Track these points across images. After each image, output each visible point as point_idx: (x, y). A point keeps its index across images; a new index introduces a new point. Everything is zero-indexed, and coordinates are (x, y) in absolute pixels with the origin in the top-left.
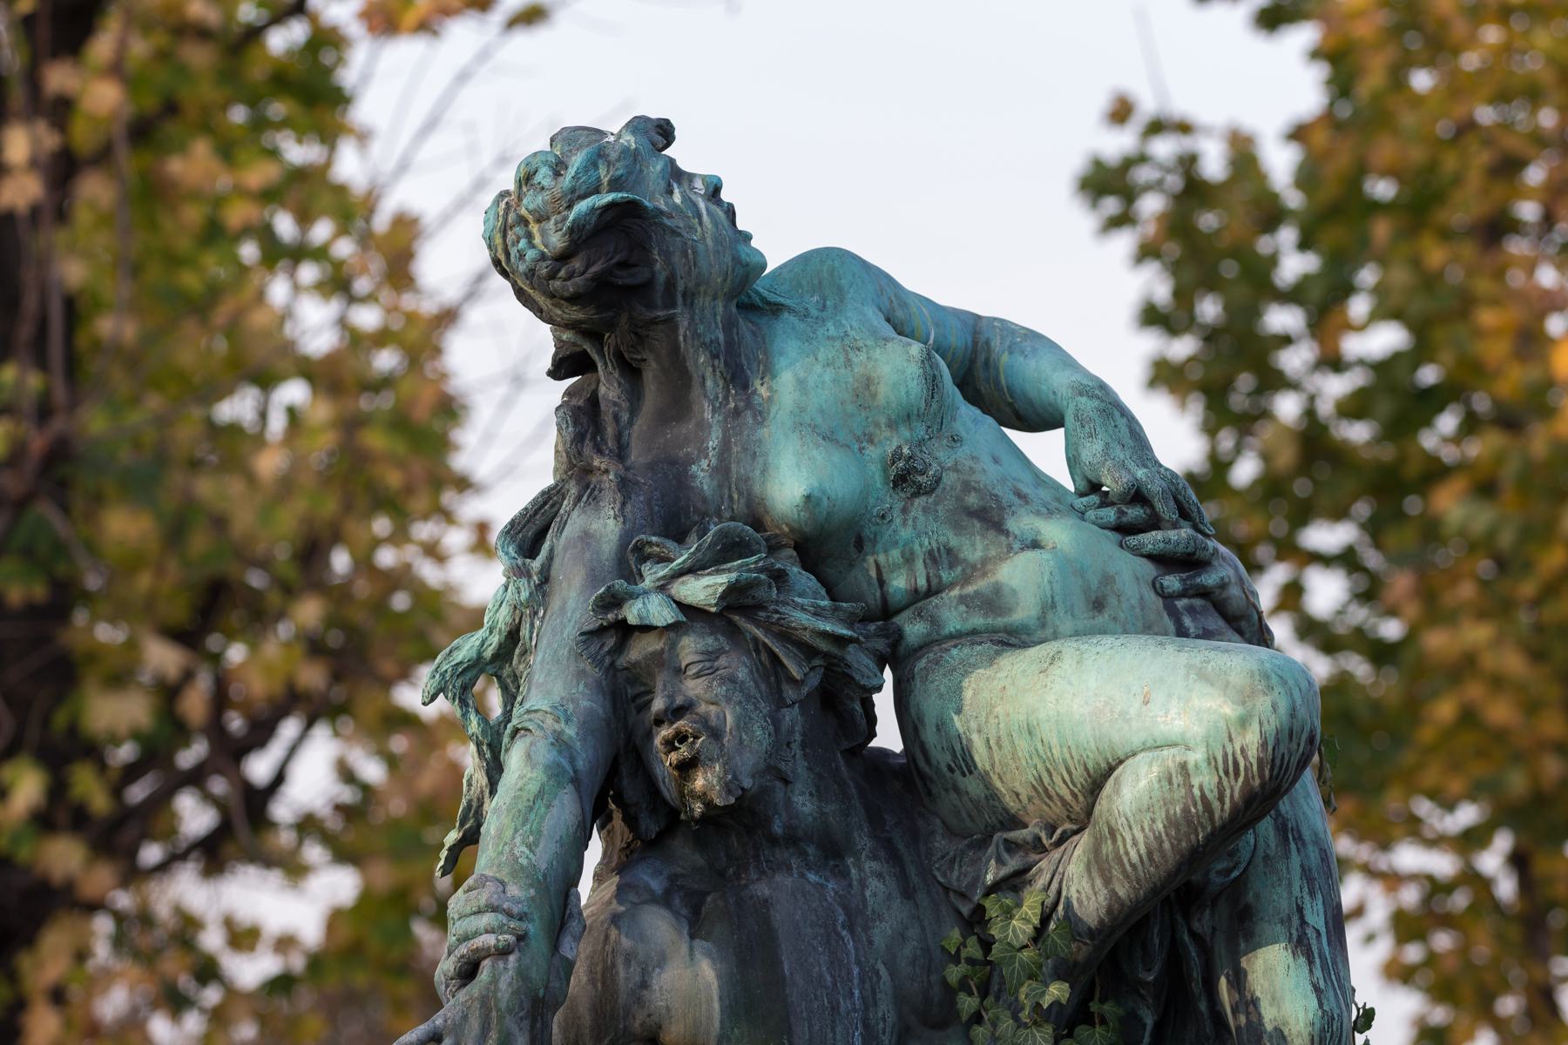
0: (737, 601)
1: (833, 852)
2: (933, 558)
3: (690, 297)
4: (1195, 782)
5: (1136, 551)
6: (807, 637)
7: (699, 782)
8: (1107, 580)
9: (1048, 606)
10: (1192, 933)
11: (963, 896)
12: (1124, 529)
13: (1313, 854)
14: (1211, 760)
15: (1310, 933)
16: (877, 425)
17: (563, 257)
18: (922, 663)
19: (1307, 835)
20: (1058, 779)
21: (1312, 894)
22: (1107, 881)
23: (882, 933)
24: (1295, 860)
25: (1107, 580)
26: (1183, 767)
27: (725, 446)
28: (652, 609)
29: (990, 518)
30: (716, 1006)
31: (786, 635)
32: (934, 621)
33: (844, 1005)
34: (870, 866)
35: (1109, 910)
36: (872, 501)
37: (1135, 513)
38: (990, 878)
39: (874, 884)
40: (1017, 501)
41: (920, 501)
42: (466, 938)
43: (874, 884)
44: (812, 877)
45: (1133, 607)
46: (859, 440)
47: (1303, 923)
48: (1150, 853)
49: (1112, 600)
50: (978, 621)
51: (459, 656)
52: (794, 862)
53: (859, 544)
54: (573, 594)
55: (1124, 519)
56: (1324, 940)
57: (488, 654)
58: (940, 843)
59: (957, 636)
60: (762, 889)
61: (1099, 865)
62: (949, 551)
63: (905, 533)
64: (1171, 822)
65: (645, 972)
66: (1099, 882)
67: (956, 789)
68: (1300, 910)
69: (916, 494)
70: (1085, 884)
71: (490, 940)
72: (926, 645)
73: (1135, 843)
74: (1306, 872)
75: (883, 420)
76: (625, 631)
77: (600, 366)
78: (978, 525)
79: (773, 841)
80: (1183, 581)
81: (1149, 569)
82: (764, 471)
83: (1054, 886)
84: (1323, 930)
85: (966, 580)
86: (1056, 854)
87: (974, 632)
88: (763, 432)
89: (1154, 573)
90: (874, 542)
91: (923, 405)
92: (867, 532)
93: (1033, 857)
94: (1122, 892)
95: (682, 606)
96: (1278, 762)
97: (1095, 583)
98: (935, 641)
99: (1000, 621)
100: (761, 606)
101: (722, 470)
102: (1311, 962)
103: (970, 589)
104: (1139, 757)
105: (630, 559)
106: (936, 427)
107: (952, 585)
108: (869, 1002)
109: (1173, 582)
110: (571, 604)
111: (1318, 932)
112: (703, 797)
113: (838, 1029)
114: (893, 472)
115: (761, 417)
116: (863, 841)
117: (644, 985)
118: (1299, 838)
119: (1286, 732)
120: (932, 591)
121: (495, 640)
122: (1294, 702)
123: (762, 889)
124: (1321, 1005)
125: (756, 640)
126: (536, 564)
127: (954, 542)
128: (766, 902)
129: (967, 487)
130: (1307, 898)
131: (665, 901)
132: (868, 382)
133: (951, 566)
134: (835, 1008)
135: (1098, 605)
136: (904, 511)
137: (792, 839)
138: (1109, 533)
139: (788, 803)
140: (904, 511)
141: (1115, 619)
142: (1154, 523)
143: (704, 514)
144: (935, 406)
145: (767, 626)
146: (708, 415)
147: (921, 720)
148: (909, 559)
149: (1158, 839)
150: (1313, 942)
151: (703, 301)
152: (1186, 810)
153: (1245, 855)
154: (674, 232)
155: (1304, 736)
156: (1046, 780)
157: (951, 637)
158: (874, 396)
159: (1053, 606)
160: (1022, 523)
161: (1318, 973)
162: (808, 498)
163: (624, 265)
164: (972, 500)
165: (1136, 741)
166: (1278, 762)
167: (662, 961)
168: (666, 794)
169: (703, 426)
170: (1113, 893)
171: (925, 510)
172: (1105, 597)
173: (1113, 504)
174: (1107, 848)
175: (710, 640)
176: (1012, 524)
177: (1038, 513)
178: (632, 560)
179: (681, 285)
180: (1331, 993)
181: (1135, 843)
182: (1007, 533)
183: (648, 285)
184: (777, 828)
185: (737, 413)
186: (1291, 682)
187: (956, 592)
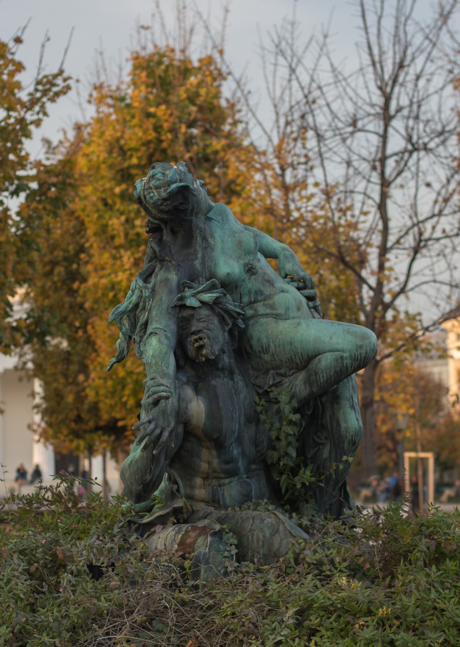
0: (217, 302)
1: (231, 373)
2: (256, 293)
3: (197, 214)
4: (345, 362)
5: (302, 294)
6: (233, 313)
7: (204, 352)
8: (300, 302)
9: (287, 309)
10: (321, 401)
11: (260, 387)
12: (299, 289)
14: (351, 356)
17: (165, 200)
18: (252, 322)
20: (297, 357)
22: (311, 387)
23: (242, 396)
26: (342, 358)
27: (203, 257)
28: (192, 302)
31: (227, 311)
32: (256, 310)
33: (235, 416)
34: (239, 377)
35: (309, 395)
37: (301, 284)
38: (271, 383)
39: (240, 382)
41: (253, 277)
42: (155, 393)
43: (240, 382)
44: (226, 380)
48: (327, 380)
50: (268, 311)
51: (120, 310)
52: (222, 375)
53: (236, 287)
54: (164, 295)
57: (129, 309)
58: (251, 372)
59: (262, 315)
60: (214, 382)
61: (308, 381)
62: (261, 291)
63: (250, 285)
64: (336, 372)
65: (187, 404)
66: (308, 387)
67: (260, 358)
70: (303, 387)
71: (164, 394)
72: (252, 317)
73: (323, 377)
76: (184, 307)
77: (165, 231)
78: (268, 284)
79: (218, 369)
82: (215, 265)
83: (290, 387)
85: (265, 300)
86: (292, 378)
87: (267, 314)
88: (214, 254)
90: (240, 287)
92: (239, 284)
93: (283, 378)
94: (315, 390)
95: (201, 302)
98: (256, 316)
99: (274, 312)
100: (220, 303)
101: (203, 263)
103: (266, 302)
104: (327, 354)
105: (181, 287)
107: (260, 301)
108: (240, 416)
110: (164, 298)
112: (205, 356)
114: (247, 268)
115: (212, 249)
116: (237, 371)
117: (186, 408)
120: (255, 302)
121: (131, 306)
123: (214, 382)
125: (219, 312)
126: (150, 286)
127: (262, 289)
128: (215, 386)
131: (187, 383)
133: (261, 295)
134: (232, 417)
136: (249, 279)
137: (223, 369)
140: (249, 279)
143: (198, 276)
145: (222, 309)
146: (197, 248)
147: (251, 338)
149: (331, 377)
151: (200, 216)
152: (341, 369)
154: (195, 196)
156: (293, 357)
157: (260, 315)
162: (228, 274)
163: (181, 204)
165: (327, 349)
167: (191, 401)
168: (190, 354)
169: (196, 251)
170: (312, 390)
171: (255, 279)
173: (295, 281)
174: (313, 378)
176: (276, 285)
178: (181, 287)
179: (195, 210)
181: (323, 377)
182: (275, 287)
183: (186, 210)
184: (220, 366)
185: (206, 248)
187: (262, 303)
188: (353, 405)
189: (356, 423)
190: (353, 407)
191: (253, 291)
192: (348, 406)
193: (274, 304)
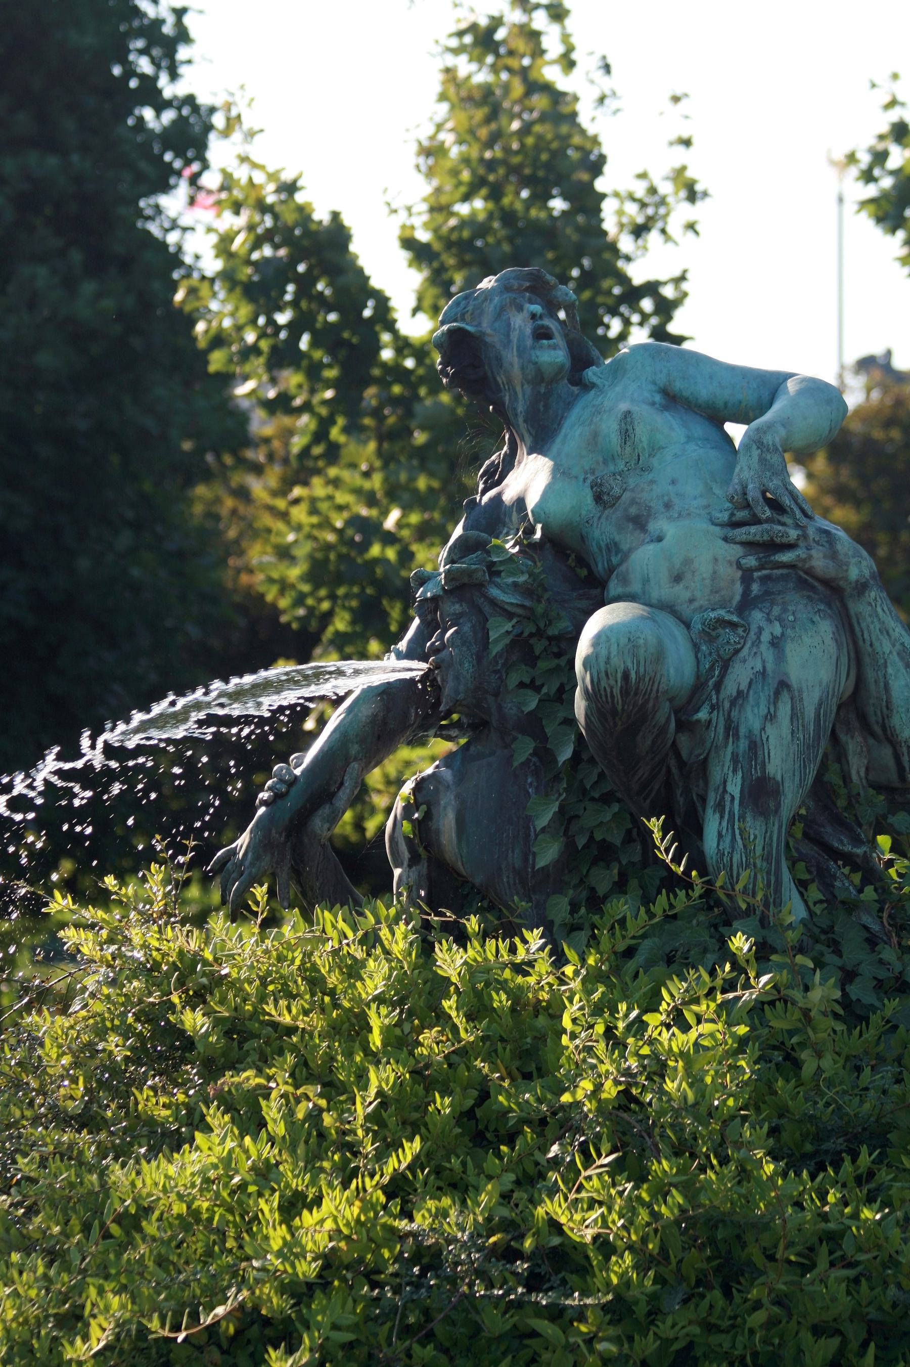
8: (687, 562)
13: (743, 744)
15: (728, 798)
16: (598, 463)
19: (743, 731)
21: (735, 771)
24: (730, 748)
25: (687, 562)
29: (639, 522)
30: (454, 835)
36: (584, 513)
37: (741, 515)
40: (662, 510)
45: (704, 579)
46: (586, 473)
47: (725, 791)
49: (688, 575)
50: (620, 590)
55: (734, 519)
56: (737, 802)
62: (616, 544)
68: (725, 782)
69: (605, 508)
74: (735, 759)
75: (601, 459)
78: (631, 526)
80: (759, 559)
81: (738, 550)
84: (737, 796)
89: (741, 554)
91: (619, 449)
96: (602, 692)
97: (677, 566)
99: (628, 590)
102: (722, 817)
106: (633, 463)
109: (751, 561)
111: (733, 798)
113: (516, 851)
118: (737, 736)
119: (603, 675)
122: (609, 653)
124: (718, 845)
127: (617, 538)
129: (633, 502)
130: (731, 774)
132: (595, 435)
133: (616, 554)
135: (678, 578)
136: (599, 518)
138: (718, 529)
139: (500, 708)
140: (599, 518)
141: (687, 588)
142: (755, 521)
144: (628, 449)
148: (600, 549)
150: (728, 804)
153: (708, 745)
155: (619, 675)
158: (596, 443)
159: (648, 580)
160: (658, 525)
161: (724, 824)
164: (633, 511)
166: (602, 692)
172: (683, 573)
175: (457, 606)
176: (654, 526)
177: (670, 518)
180: (729, 837)
186: (613, 640)
188: (723, 798)
189: (715, 845)
190: (720, 807)
191: (603, 545)
192: (712, 803)
193: (627, 570)
